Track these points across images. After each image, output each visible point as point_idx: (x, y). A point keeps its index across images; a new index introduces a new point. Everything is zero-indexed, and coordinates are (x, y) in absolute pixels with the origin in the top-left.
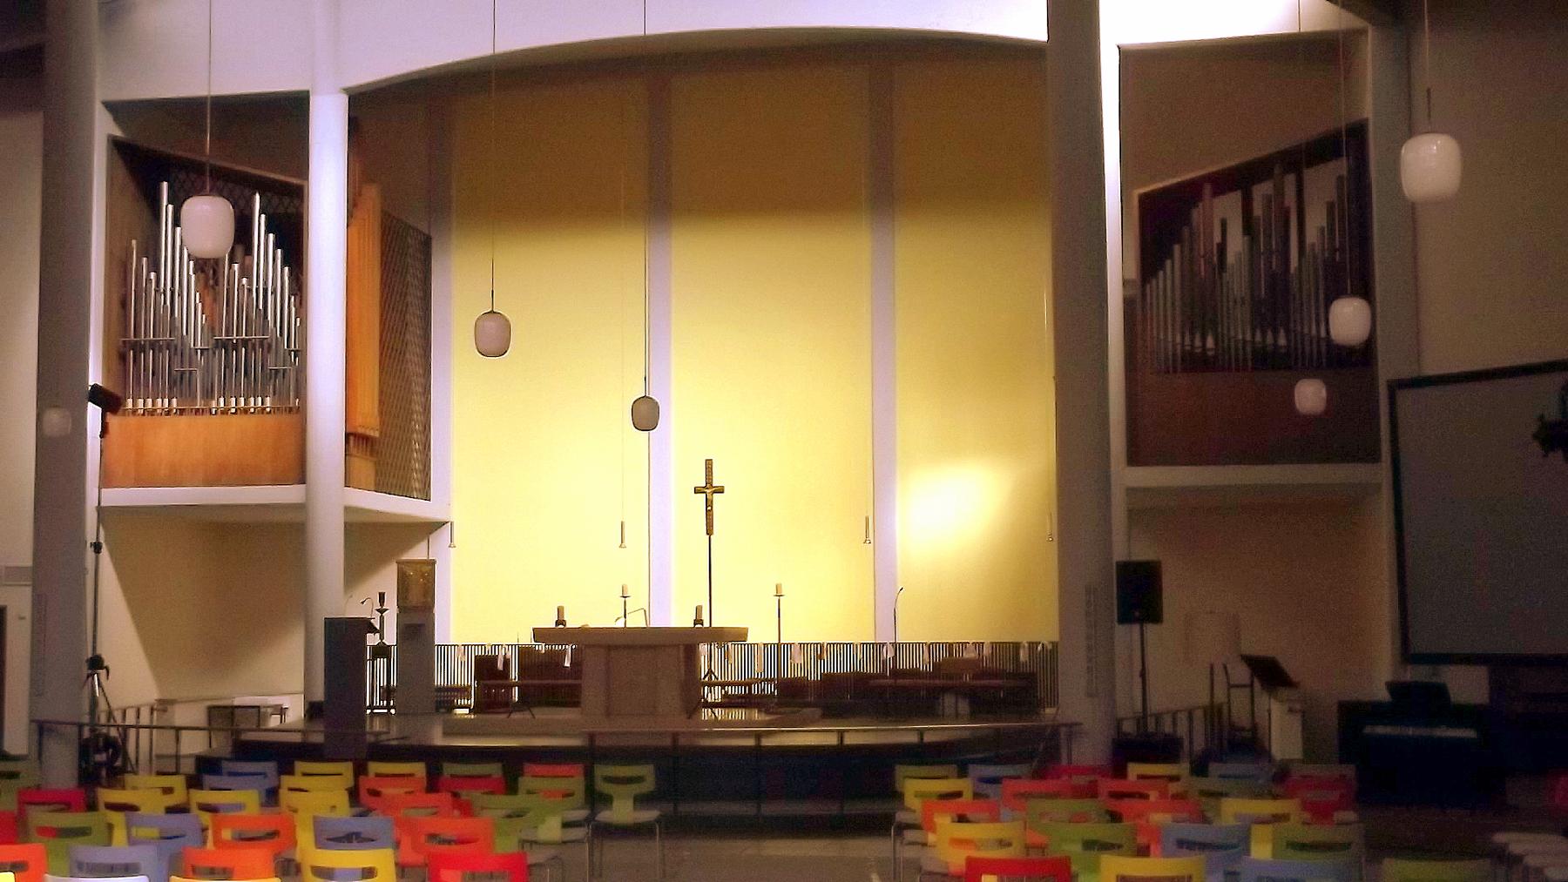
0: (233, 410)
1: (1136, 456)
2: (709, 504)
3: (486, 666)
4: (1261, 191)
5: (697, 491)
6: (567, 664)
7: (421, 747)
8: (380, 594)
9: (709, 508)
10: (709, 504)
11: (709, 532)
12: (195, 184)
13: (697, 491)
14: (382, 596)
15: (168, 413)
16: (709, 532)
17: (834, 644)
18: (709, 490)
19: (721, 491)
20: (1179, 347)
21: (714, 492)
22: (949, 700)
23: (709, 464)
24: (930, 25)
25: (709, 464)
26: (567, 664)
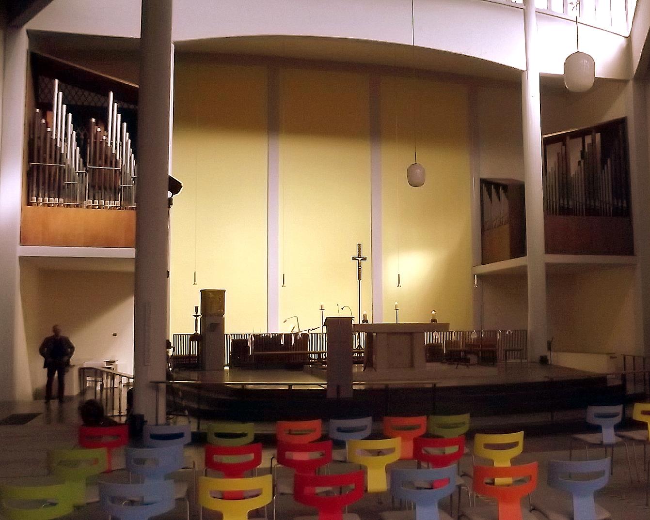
0: (97, 207)
1: (551, 247)
2: (359, 265)
3: (239, 344)
4: (588, 140)
5: (354, 259)
6: (282, 343)
7: (216, 385)
8: (196, 307)
9: (360, 267)
10: (359, 265)
11: (359, 279)
12: (68, 92)
13: (354, 259)
14: (197, 308)
15: (58, 206)
16: (359, 279)
17: (177, 335)
18: (359, 258)
19: (365, 259)
20: (558, 205)
21: (362, 260)
22: (473, 358)
23: (359, 246)
24: (467, 53)
25: (359, 246)
26: (282, 343)
